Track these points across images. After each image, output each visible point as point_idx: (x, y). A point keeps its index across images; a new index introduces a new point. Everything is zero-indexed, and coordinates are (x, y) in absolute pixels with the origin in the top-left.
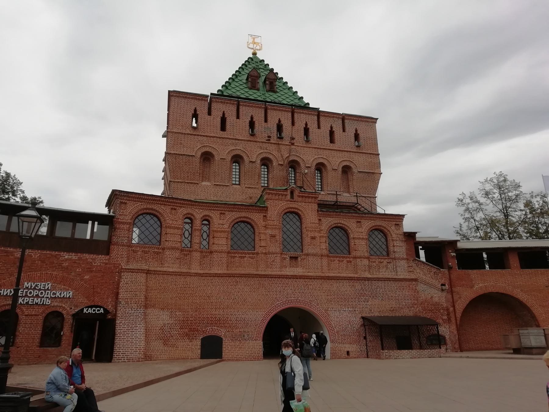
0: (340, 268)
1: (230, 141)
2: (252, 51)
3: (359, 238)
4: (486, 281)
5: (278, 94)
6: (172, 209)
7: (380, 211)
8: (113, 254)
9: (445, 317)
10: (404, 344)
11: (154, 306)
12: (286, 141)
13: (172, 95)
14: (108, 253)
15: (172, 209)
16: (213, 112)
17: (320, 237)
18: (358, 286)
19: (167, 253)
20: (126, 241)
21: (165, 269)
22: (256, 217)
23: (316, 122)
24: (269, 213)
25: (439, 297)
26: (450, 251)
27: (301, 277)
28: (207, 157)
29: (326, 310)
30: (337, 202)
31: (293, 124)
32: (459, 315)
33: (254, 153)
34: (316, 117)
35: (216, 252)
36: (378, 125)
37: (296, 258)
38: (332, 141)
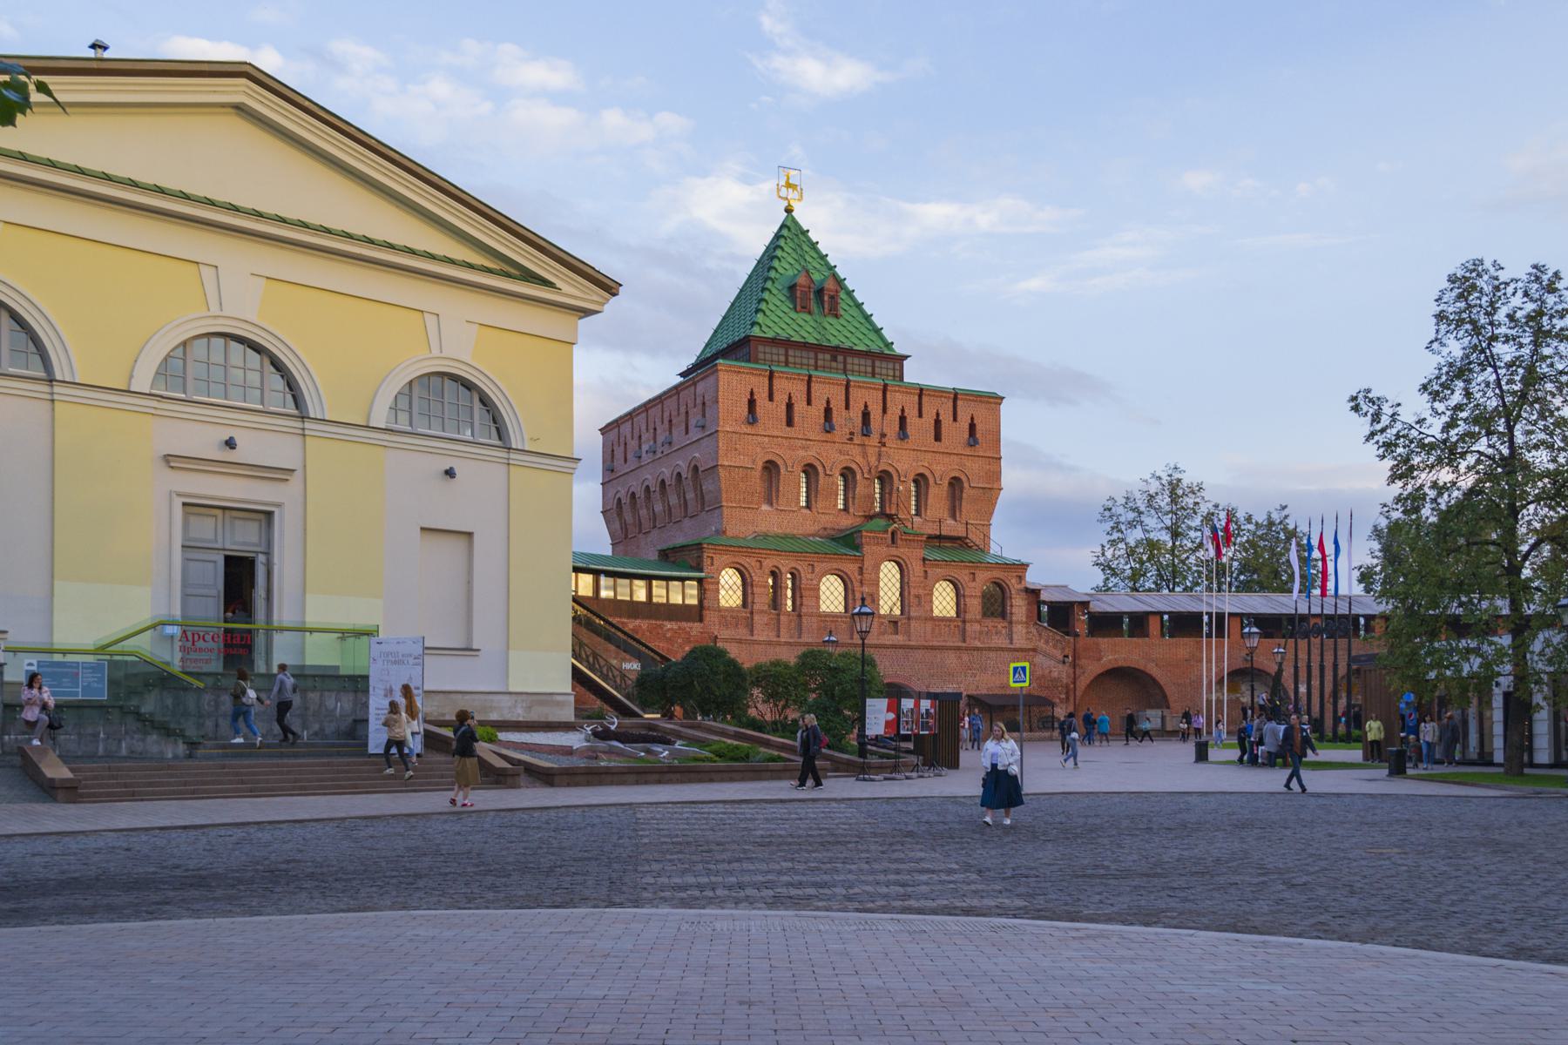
1: (799, 443)
2: (785, 204)
4: (1117, 651)
5: (842, 321)
8: (707, 619)
14: (701, 620)
16: (777, 396)
18: (965, 658)
24: (866, 564)
25: (1061, 672)
27: (901, 647)
28: (771, 468)
31: (885, 410)
38: (938, 438)
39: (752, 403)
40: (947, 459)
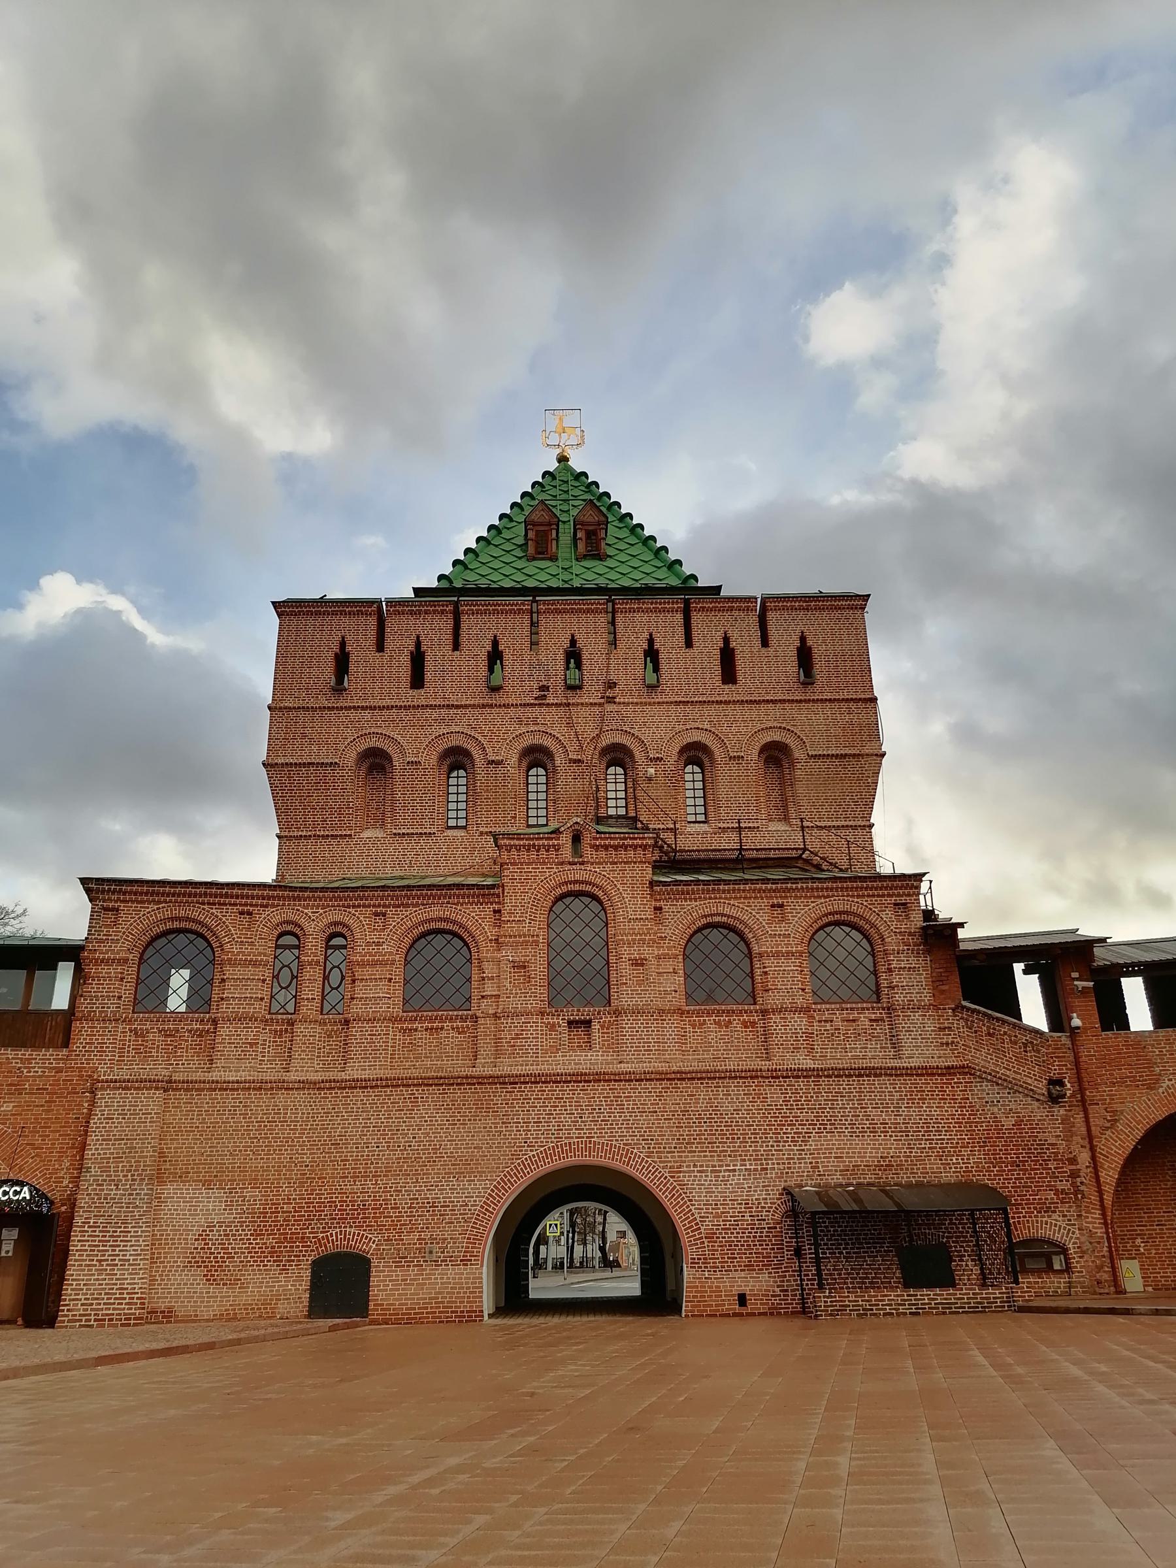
0: (722, 1042)
1: (435, 714)
3: (777, 955)
5: (610, 563)
6: (242, 913)
8: (79, 1042)
9: (1064, 1185)
10: (927, 1268)
11: (182, 1177)
12: (592, 693)
15: (242, 913)
17: (659, 957)
18: (774, 1093)
19: (224, 1030)
20: (113, 1008)
21: (215, 1076)
22: (474, 917)
23: (681, 631)
26: (1075, 975)
27: (599, 1078)
28: (376, 762)
29: (675, 1172)
30: (741, 850)
32: (1110, 1176)
33: (500, 738)
34: (679, 617)
35: (358, 1019)
37: (588, 1023)
39: (342, 663)
40: (753, 712)
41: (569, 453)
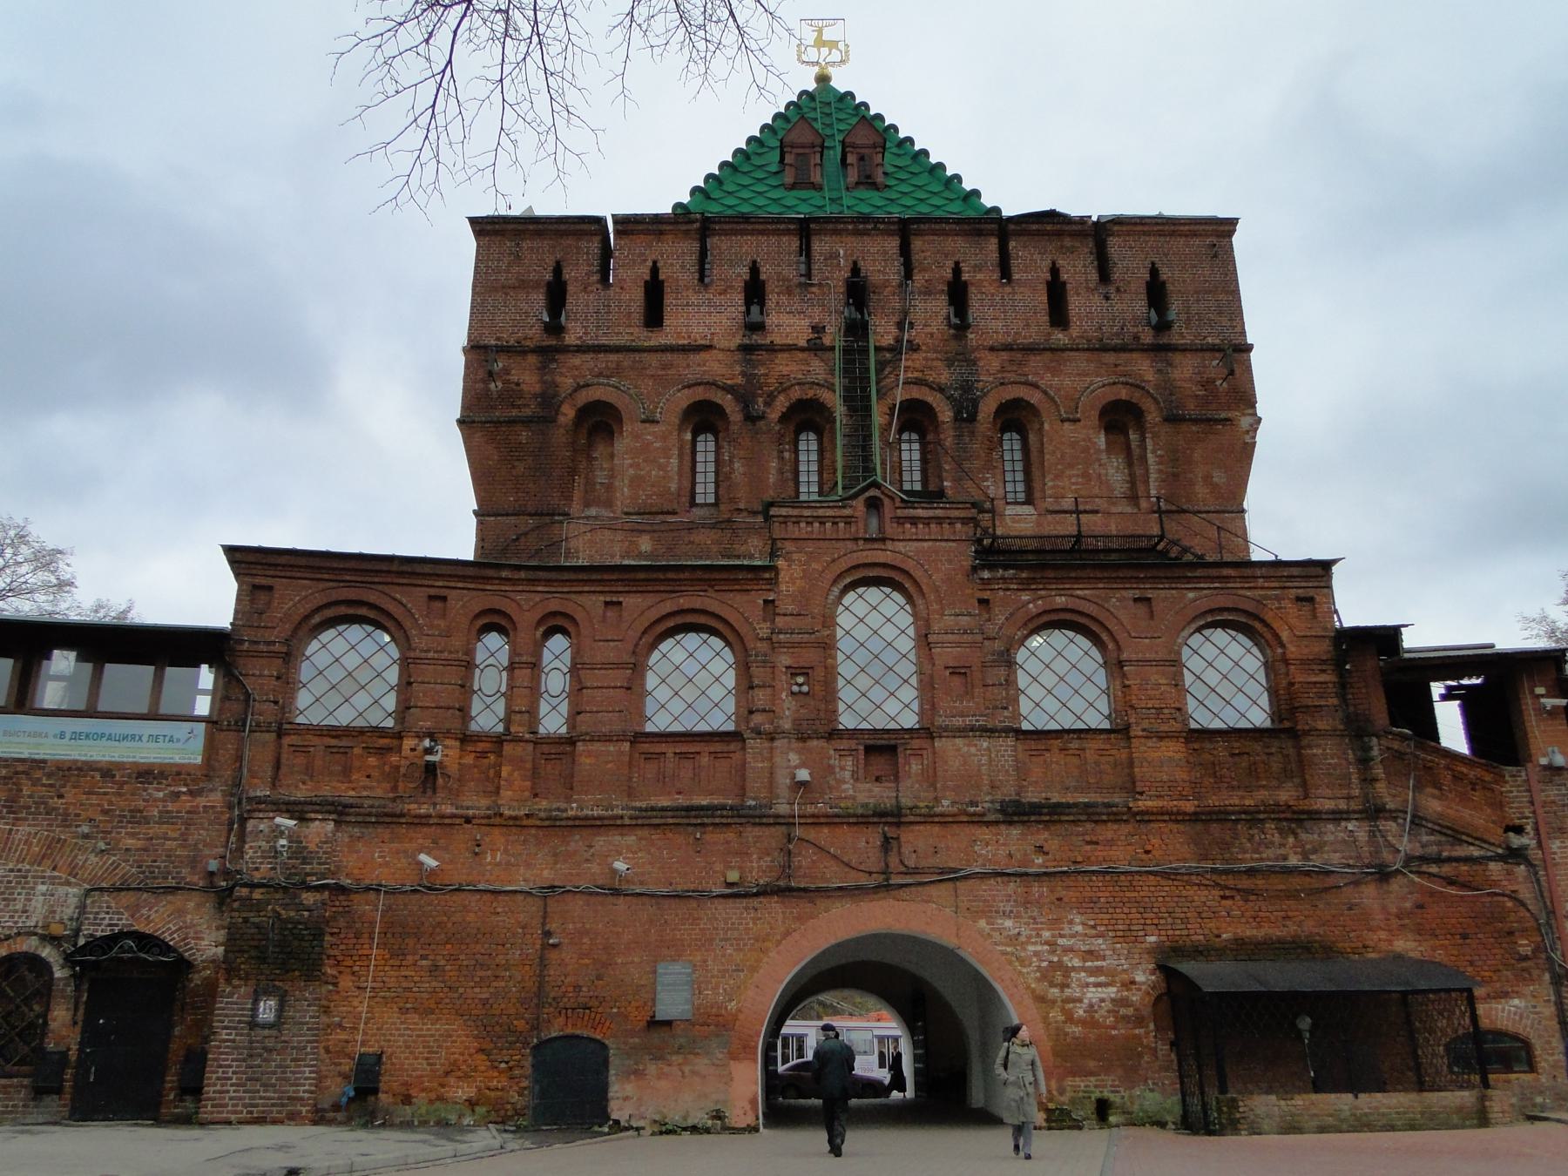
5: (887, 194)
7: (1257, 555)
13: (485, 227)
26: (1540, 690)
30: (1079, 537)
36: (1240, 242)
41: (832, 71)
